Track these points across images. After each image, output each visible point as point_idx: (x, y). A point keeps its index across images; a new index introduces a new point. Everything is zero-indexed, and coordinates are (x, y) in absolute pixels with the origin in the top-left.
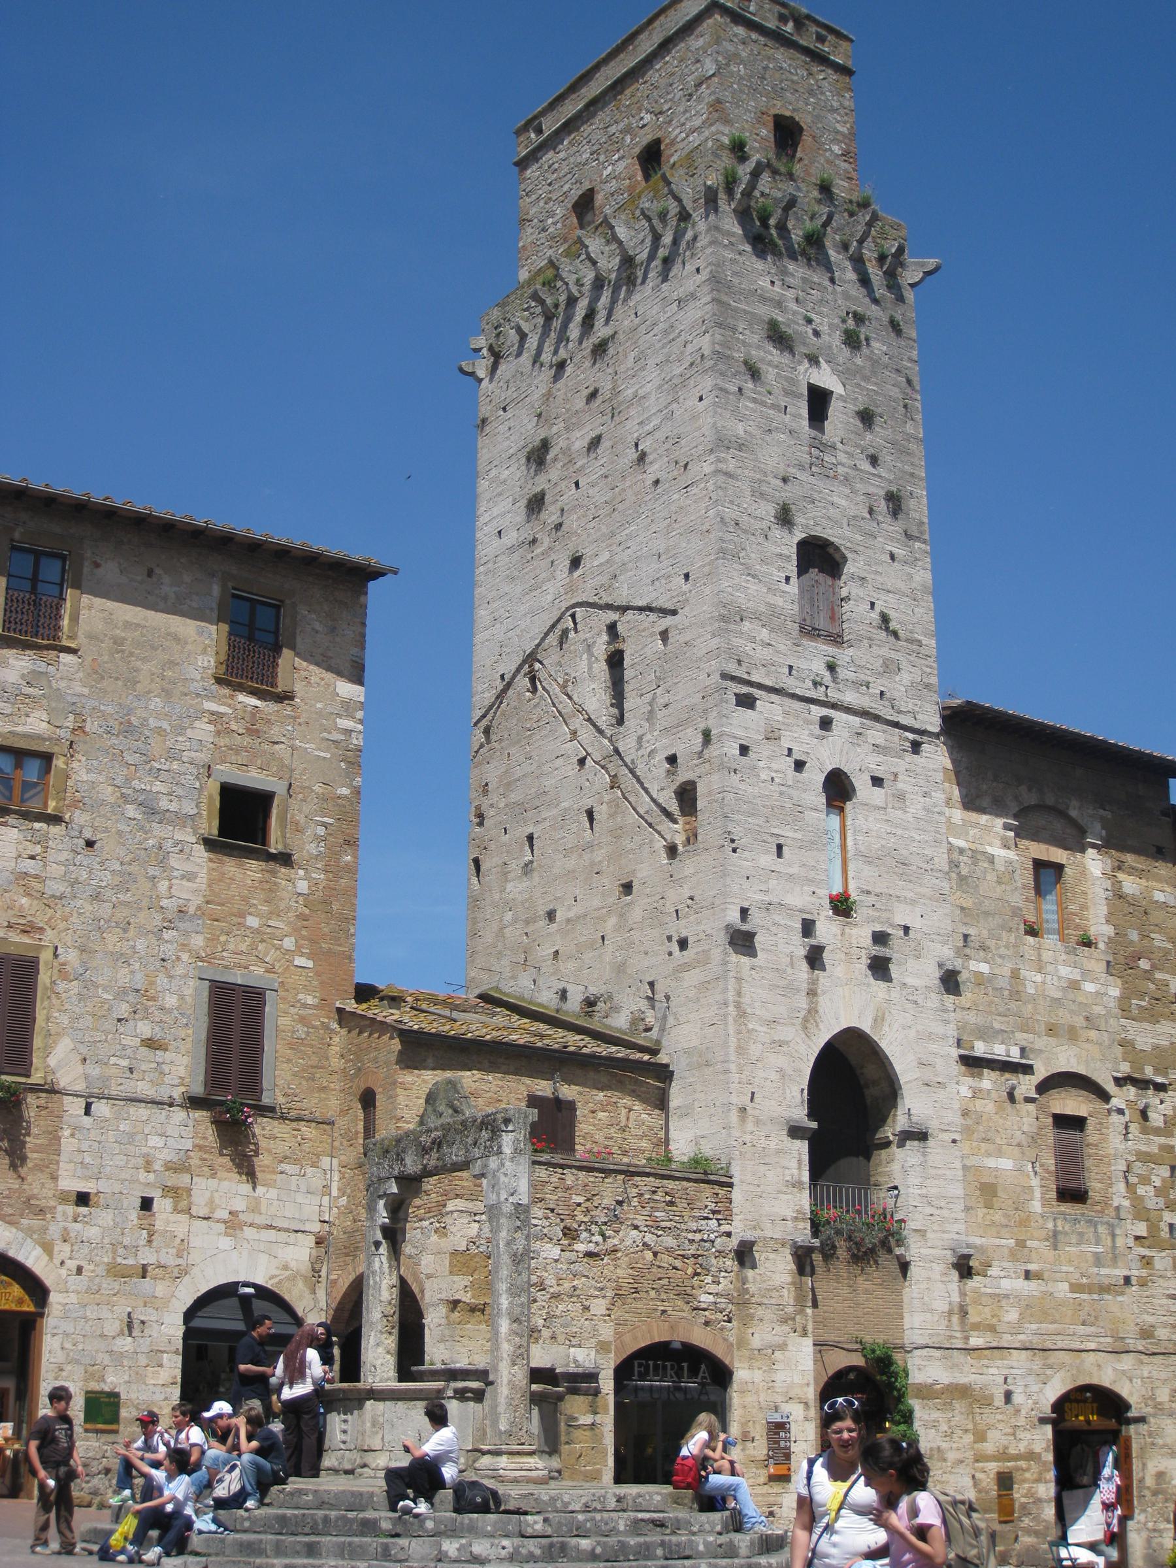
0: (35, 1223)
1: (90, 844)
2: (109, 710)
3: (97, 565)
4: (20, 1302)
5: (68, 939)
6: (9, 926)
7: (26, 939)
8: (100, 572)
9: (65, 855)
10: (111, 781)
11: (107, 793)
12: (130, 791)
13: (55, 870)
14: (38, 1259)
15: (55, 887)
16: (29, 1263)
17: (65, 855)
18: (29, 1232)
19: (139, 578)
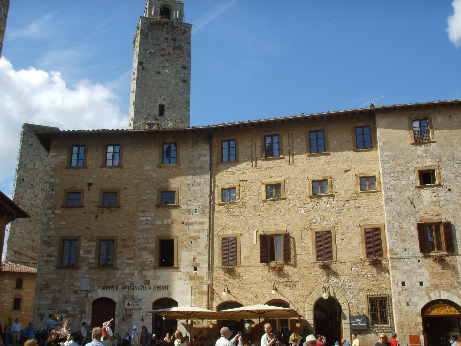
0: (455, 290)
1: (450, 190)
2: (447, 154)
3: (435, 119)
4: (455, 312)
5: (449, 216)
6: (432, 215)
7: (437, 218)
8: (436, 120)
9: (443, 194)
10: (452, 173)
11: (452, 176)
12: (458, 174)
13: (442, 198)
14: (457, 300)
15: (443, 203)
16: (455, 301)
17: (443, 194)
18: (454, 293)
19: (447, 119)
